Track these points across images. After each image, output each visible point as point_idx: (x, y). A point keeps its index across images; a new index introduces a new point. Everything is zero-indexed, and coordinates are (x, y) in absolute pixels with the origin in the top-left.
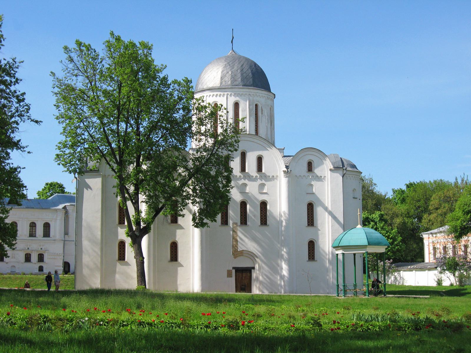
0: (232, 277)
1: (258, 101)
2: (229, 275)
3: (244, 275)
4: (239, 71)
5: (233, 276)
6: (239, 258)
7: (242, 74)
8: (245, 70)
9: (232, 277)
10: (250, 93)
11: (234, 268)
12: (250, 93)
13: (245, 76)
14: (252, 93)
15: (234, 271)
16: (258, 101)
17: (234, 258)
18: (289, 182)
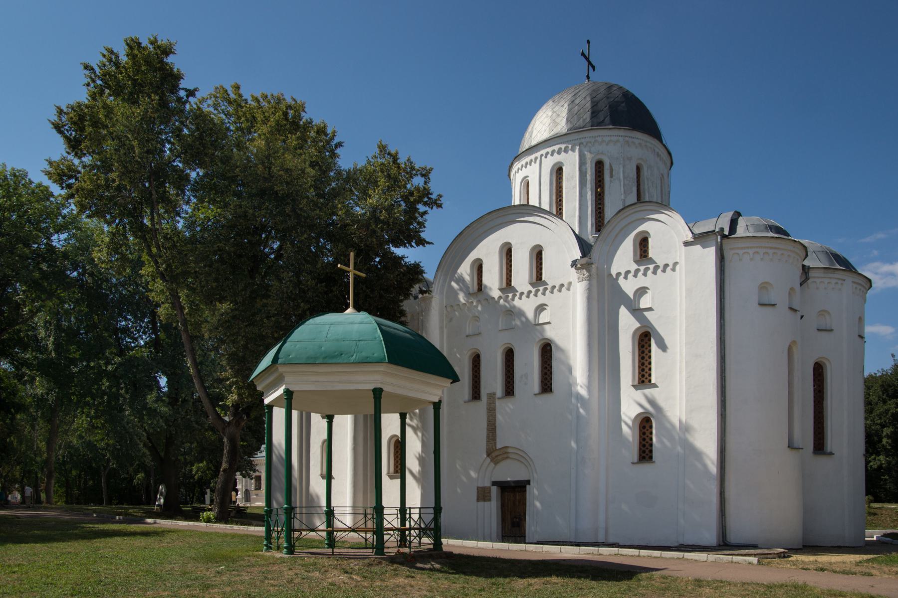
0: (490, 500)
1: (602, 153)
2: (483, 495)
3: (518, 498)
4: (566, 106)
5: (492, 499)
6: (503, 464)
7: (570, 110)
8: (577, 102)
9: (490, 500)
10: (583, 140)
11: (494, 483)
12: (583, 140)
13: (576, 112)
14: (587, 140)
15: (494, 489)
16: (602, 153)
17: (492, 465)
18: (589, 290)
